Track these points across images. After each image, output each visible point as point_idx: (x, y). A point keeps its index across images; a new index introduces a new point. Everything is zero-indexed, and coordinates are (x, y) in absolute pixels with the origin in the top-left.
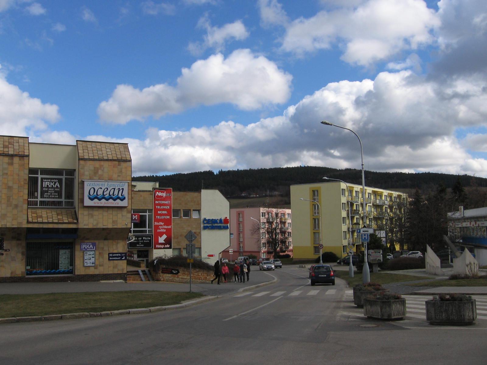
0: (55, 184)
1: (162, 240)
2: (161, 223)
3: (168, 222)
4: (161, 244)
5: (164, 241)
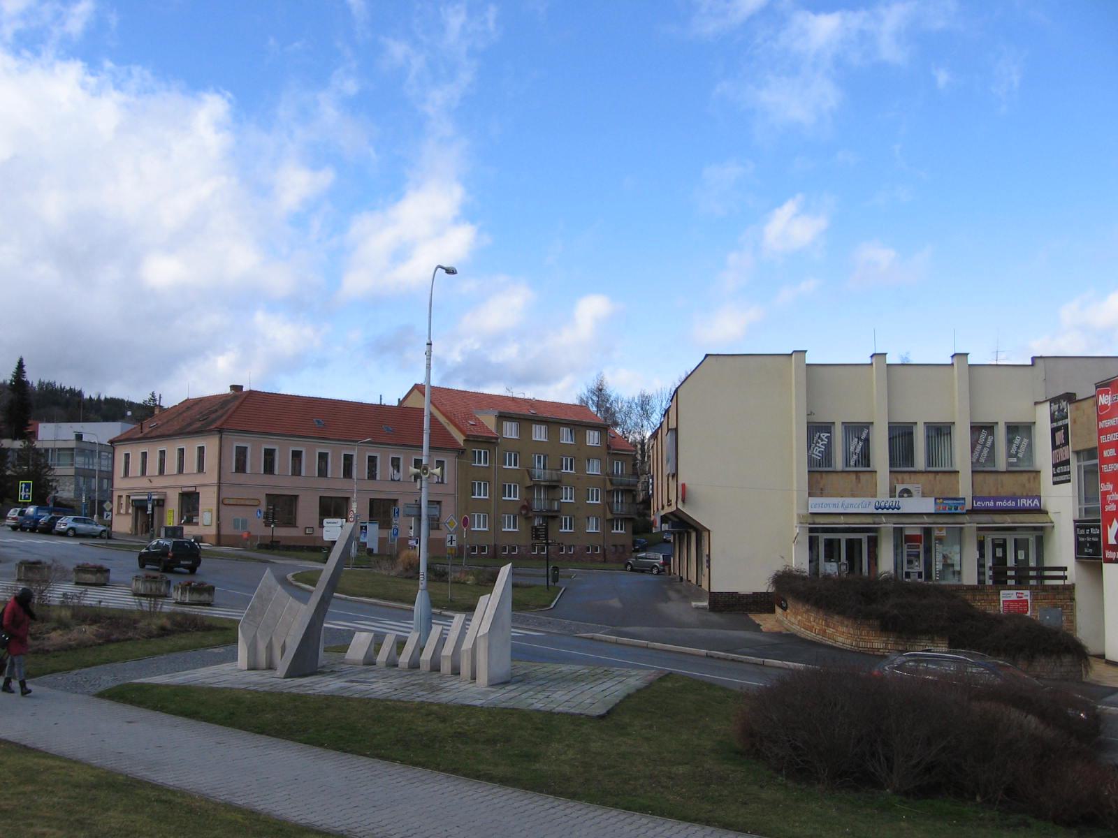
0: (1033, 502)
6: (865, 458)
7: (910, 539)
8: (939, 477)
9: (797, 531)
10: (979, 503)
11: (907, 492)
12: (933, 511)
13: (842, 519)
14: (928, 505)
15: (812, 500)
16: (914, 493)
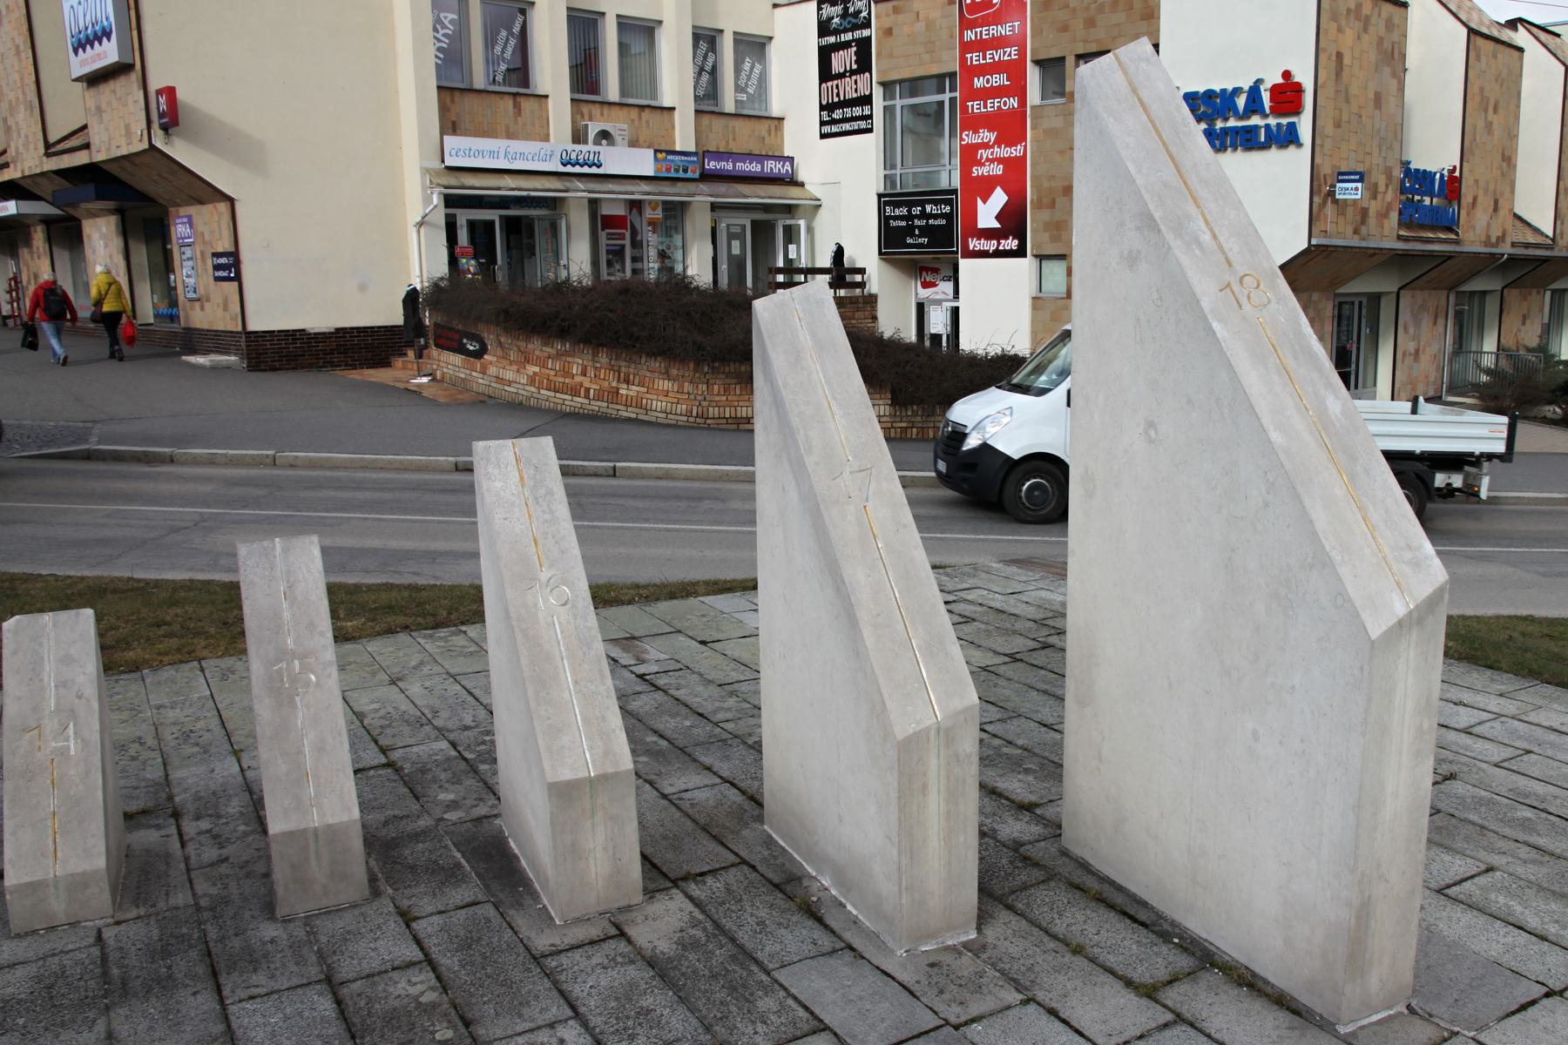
1: (988, 214)
2: (987, 136)
3: (1010, 128)
4: (988, 234)
5: (997, 218)
6: (520, 72)
7: (610, 222)
8: (646, 114)
9: (417, 201)
10: (712, 164)
11: (604, 135)
12: (652, 174)
13: (509, 181)
14: (643, 162)
15: (451, 141)
16: (618, 139)
